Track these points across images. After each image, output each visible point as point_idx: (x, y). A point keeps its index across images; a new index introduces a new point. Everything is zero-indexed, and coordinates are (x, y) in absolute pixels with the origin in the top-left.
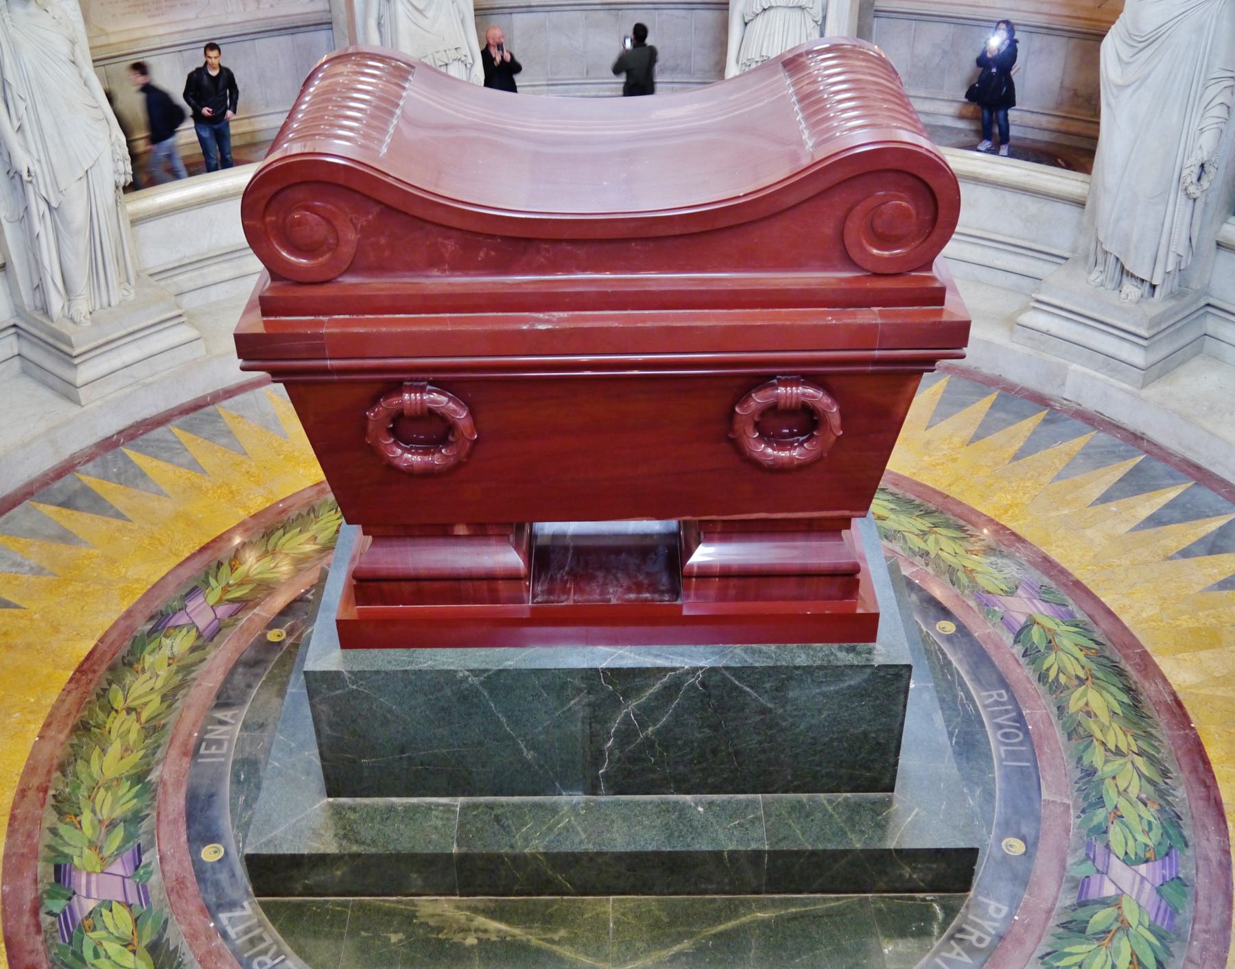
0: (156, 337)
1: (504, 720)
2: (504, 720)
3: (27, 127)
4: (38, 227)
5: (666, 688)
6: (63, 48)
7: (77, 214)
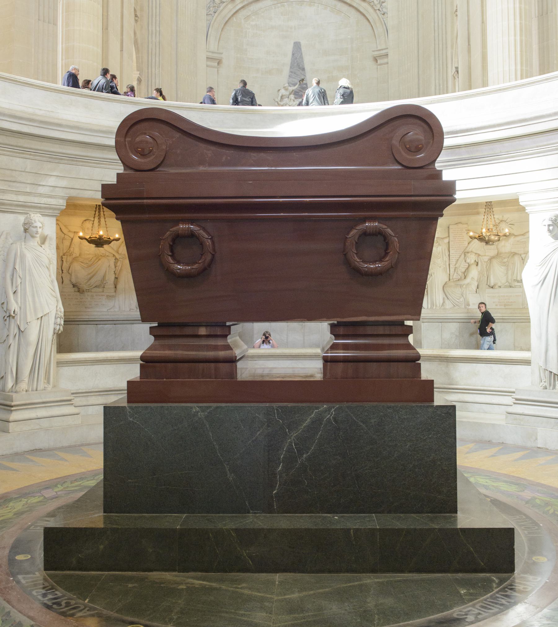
0: (57, 408)
1: (217, 447)
2: (217, 447)
3: (19, 291)
4: (11, 340)
5: (313, 422)
6: (46, 261)
7: (33, 335)
